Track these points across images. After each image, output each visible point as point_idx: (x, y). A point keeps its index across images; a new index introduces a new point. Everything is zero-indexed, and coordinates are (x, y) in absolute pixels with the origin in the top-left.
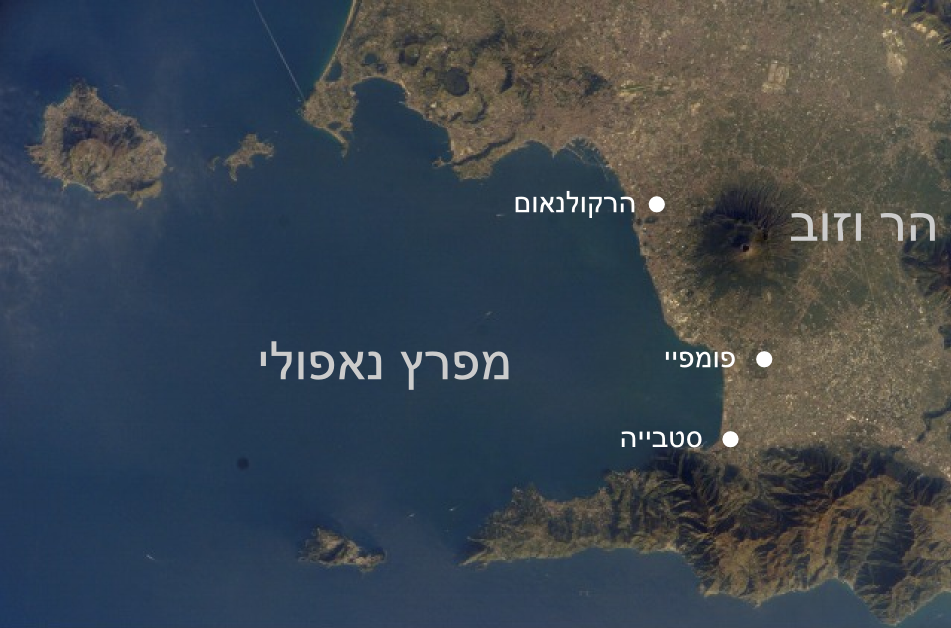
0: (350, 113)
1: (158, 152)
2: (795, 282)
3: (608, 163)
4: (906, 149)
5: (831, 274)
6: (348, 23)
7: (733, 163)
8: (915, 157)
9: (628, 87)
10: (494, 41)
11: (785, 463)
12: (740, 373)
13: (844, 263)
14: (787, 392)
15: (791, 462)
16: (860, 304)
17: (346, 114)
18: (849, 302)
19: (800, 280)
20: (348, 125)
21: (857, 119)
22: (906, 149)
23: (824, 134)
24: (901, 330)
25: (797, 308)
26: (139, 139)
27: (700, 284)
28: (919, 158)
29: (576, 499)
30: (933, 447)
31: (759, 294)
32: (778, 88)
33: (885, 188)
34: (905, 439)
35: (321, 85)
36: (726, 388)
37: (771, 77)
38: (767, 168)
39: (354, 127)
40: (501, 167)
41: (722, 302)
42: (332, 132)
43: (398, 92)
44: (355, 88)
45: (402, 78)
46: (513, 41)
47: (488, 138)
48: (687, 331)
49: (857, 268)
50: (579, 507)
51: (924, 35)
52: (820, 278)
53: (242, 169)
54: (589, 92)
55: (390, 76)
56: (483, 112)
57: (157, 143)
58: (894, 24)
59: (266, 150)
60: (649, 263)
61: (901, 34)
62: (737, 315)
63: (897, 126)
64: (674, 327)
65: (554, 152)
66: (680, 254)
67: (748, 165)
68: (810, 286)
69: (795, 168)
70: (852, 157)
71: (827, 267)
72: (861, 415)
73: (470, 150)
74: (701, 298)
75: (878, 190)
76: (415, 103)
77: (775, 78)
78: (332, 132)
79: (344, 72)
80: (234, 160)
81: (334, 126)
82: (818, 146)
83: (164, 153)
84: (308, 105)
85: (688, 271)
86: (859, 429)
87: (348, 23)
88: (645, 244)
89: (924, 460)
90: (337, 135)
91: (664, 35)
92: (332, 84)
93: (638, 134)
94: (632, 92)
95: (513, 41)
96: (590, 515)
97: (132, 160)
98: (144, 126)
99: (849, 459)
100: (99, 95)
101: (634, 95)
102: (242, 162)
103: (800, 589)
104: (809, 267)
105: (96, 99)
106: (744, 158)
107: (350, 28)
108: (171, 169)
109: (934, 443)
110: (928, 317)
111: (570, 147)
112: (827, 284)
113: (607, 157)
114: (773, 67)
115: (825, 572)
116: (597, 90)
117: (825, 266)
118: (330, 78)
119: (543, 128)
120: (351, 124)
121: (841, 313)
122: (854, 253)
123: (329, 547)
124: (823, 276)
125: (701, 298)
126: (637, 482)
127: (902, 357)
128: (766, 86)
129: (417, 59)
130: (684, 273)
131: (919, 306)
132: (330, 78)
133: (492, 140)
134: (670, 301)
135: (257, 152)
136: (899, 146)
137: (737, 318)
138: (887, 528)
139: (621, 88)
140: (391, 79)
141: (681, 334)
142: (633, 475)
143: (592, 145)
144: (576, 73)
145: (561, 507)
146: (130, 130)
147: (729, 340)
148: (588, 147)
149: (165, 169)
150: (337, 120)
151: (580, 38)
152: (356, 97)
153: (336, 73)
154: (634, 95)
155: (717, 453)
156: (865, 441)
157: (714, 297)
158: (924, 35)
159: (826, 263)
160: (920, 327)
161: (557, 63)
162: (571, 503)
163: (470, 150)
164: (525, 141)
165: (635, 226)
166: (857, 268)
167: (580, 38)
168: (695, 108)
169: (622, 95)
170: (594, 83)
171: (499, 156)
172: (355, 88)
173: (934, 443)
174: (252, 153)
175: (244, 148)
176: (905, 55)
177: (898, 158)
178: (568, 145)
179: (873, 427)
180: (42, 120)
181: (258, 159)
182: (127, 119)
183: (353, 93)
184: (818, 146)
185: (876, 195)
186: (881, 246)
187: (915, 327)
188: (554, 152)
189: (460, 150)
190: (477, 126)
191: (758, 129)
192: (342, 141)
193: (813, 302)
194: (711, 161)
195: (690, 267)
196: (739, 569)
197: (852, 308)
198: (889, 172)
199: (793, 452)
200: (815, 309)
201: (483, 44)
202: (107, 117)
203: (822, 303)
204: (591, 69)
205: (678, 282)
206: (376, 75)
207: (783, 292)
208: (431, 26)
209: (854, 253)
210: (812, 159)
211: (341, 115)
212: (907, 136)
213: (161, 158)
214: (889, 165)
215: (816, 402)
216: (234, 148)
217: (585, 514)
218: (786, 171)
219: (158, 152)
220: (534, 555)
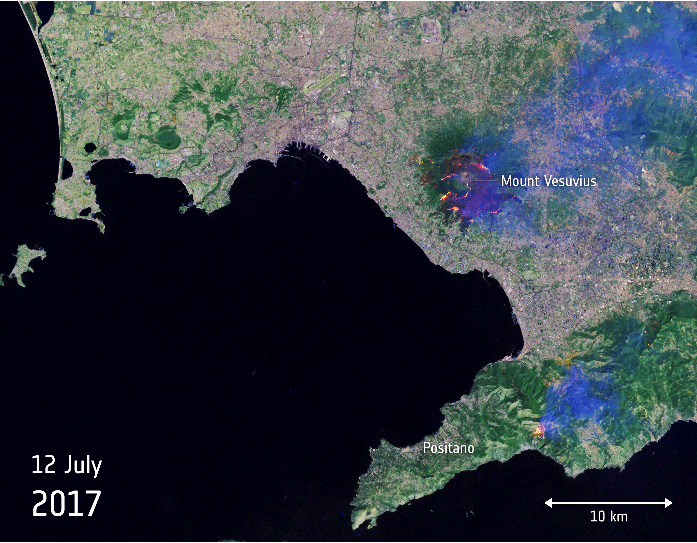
10: (182, 94)
11: (589, 341)
15: (592, 338)
20: (96, 209)
33: (565, 83)
40: (234, 191)
46: (198, 87)
53: (25, 276)
55: (112, 155)
59: (42, 254)
67: (441, 110)
74: (454, 229)
76: (143, 168)
80: (18, 271)
81: (86, 212)
90: (89, 218)
95: (198, 87)
99: (643, 316)
102: (22, 271)
103: (653, 440)
121: (577, 199)
125: (454, 229)
143: (304, 144)
153: (68, 171)
155: (528, 354)
165: (370, 195)
181: (34, 263)
189: (197, 193)
192: (97, 221)
199: (593, 330)
201: (175, 100)
210: (492, 84)
216: (13, 262)
220: (411, 497)
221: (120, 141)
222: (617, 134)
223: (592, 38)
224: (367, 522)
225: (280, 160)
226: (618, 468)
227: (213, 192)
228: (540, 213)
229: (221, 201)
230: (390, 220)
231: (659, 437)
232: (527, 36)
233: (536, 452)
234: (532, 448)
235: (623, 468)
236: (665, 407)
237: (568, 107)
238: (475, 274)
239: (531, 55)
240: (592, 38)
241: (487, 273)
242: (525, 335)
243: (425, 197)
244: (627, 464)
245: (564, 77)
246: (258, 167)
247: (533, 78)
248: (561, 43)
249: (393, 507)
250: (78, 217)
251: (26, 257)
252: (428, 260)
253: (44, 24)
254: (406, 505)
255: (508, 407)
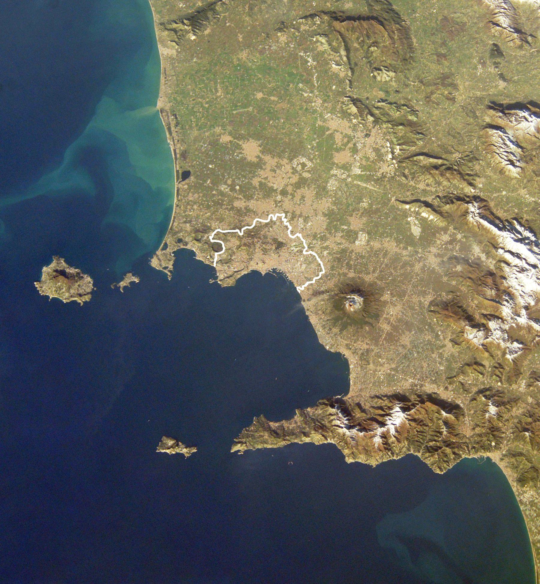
0: (172, 263)
1: (90, 283)
2: (379, 323)
3: (288, 277)
4: (425, 266)
5: (395, 319)
6: (169, 228)
7: (345, 275)
8: (429, 269)
9: (294, 246)
11: (381, 401)
12: (357, 363)
13: (401, 314)
14: (380, 371)
16: (410, 332)
17: (170, 263)
18: (405, 331)
19: (380, 322)
20: (171, 267)
21: (400, 254)
22: (425, 266)
23: (385, 260)
24: (431, 342)
25: (381, 334)
26: (82, 277)
27: (334, 325)
28: (431, 269)
29: (284, 421)
30: (452, 392)
31: (362, 328)
32: (363, 243)
33: (417, 282)
34: (438, 389)
35: (159, 252)
36: (351, 370)
37: (359, 239)
38: (361, 275)
39: (173, 268)
40: (239, 281)
41: (344, 333)
42: (164, 271)
43: (193, 253)
44: (173, 253)
45: (193, 246)
47: (232, 269)
48: (331, 346)
49: (407, 316)
50: (285, 423)
51: (427, 219)
52: (390, 321)
53: (125, 288)
54: (276, 248)
55: (189, 247)
56: (231, 259)
57: (89, 279)
58: (413, 215)
59: (137, 280)
60: (310, 318)
61: (417, 218)
62: (352, 338)
63: (420, 256)
64: (324, 344)
65: (263, 274)
66: (323, 313)
67: (351, 275)
68: (386, 324)
69: (374, 275)
70: (400, 270)
71: (393, 316)
72: (416, 380)
73: (226, 275)
74: (335, 330)
75: (413, 283)
76: (199, 257)
77: (361, 239)
78: (164, 271)
79: (169, 247)
80: (122, 284)
81: (166, 268)
82: (383, 266)
83: (92, 282)
84: (153, 260)
85: (328, 320)
86: (416, 386)
87: (169, 228)
88: (308, 310)
89: (449, 399)
90: (166, 271)
91: (309, 224)
92: (164, 251)
93: (301, 265)
94: (297, 247)
96: (291, 428)
97: (79, 286)
98: (84, 273)
100: (65, 261)
101: (298, 249)
102: (125, 284)
103: (395, 458)
104: (384, 316)
105: (64, 263)
106: (349, 272)
107: (171, 229)
108: (95, 289)
109: (452, 391)
110: (444, 336)
111: (270, 271)
112: (394, 323)
113: (288, 275)
114: (359, 235)
115: (404, 449)
116: (281, 247)
117: (392, 315)
118: (163, 249)
119: (257, 264)
120: (172, 267)
121: (402, 335)
122: (405, 309)
123: (169, 445)
124: (391, 320)
125: (335, 330)
126: (312, 412)
127: (433, 353)
128: (357, 243)
129: (201, 239)
130: (326, 321)
131: (438, 331)
132: (163, 249)
133: (236, 270)
134: (320, 332)
135: (132, 280)
136: (421, 264)
137: (353, 339)
138: (433, 428)
139: (291, 246)
140: (189, 248)
141: (327, 348)
142: (309, 409)
144: (270, 241)
145: (277, 425)
146: (78, 274)
147: (350, 349)
148: (278, 271)
149: (93, 289)
150: (167, 265)
151: (271, 227)
152: (174, 256)
153: (166, 247)
154: (298, 249)
155: (349, 398)
156: (419, 391)
157: (341, 330)
158: (427, 219)
159: (392, 314)
160: (440, 340)
161: (262, 237)
162: (282, 422)
163: (226, 275)
164: (250, 270)
165: (302, 303)
166: (407, 316)
167: (271, 227)
168: (325, 253)
169: (292, 249)
170: (280, 245)
171: (239, 276)
172: (173, 253)
173: (452, 391)
174: (130, 281)
175: (126, 279)
176: (421, 228)
177: (421, 269)
178: (269, 271)
179: (422, 384)
180: (41, 272)
182: (77, 270)
183: (173, 255)
184: (383, 266)
185: (413, 285)
186: (417, 306)
187: (438, 340)
188: (263, 274)
189: (221, 276)
190: (228, 264)
191: (355, 260)
192: (169, 274)
193: (388, 331)
194: (335, 274)
195: (328, 318)
196: (363, 448)
197: (407, 333)
198: (418, 275)
200: (389, 334)
202: (68, 269)
203: (392, 331)
204: (277, 239)
205: (325, 325)
206: (182, 247)
207: (373, 327)
208: (205, 226)
209: (405, 309)
210: (381, 271)
211: (168, 263)
212: (424, 260)
213: (91, 285)
214: (417, 272)
215: (394, 375)
216: (122, 279)
217: (288, 427)
218: (370, 276)
219: (90, 283)
221: (194, 241)
222: (431, 311)
223: (438, 266)
224: (239, 451)
225: (266, 274)
226: (372, 466)
227: (228, 277)
228: (381, 336)
229: (230, 282)
230: (307, 316)
231: (398, 458)
232: (407, 255)
233: (335, 445)
234: (333, 443)
235: (375, 466)
236: (406, 443)
237: (414, 292)
238: (338, 355)
239: (405, 264)
240: (438, 266)
241: (344, 355)
242: (351, 389)
243: (328, 311)
244: (377, 465)
245: (417, 278)
246: (255, 273)
247: (402, 275)
248: (421, 264)
249: (254, 448)
250: (161, 269)
251: (131, 279)
252: (318, 339)
253: (183, 180)
254: (261, 449)
255: (329, 418)
